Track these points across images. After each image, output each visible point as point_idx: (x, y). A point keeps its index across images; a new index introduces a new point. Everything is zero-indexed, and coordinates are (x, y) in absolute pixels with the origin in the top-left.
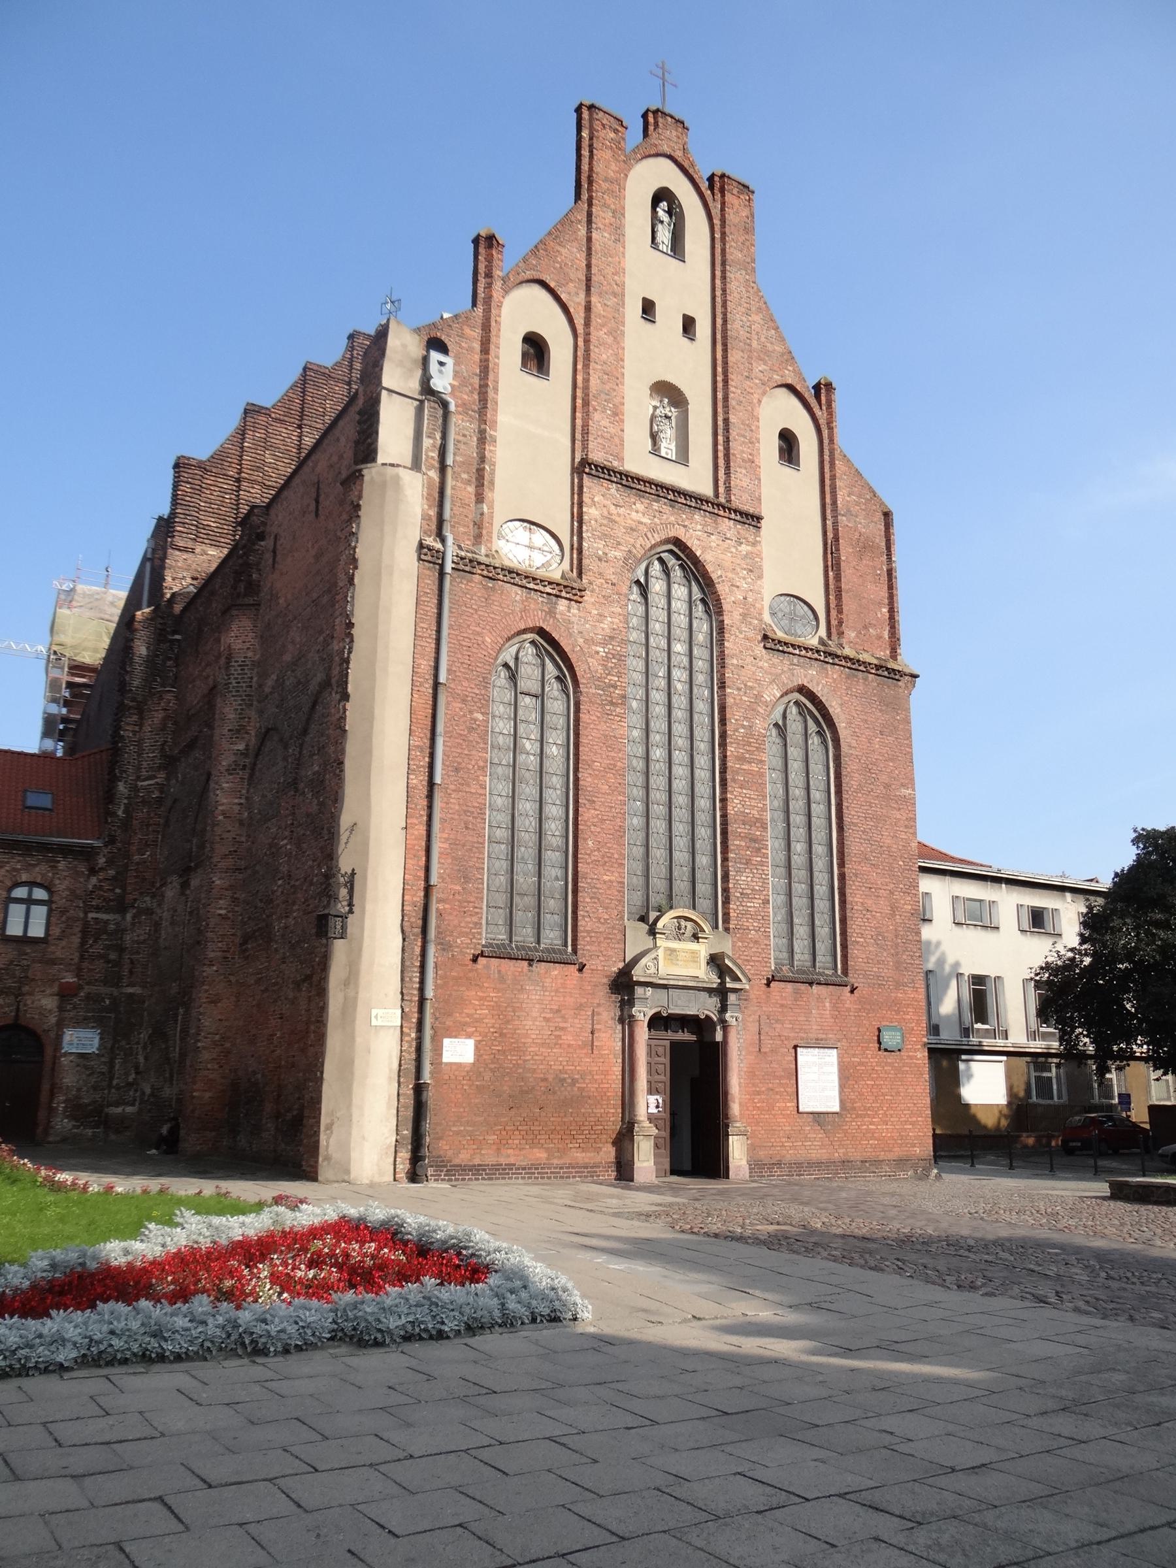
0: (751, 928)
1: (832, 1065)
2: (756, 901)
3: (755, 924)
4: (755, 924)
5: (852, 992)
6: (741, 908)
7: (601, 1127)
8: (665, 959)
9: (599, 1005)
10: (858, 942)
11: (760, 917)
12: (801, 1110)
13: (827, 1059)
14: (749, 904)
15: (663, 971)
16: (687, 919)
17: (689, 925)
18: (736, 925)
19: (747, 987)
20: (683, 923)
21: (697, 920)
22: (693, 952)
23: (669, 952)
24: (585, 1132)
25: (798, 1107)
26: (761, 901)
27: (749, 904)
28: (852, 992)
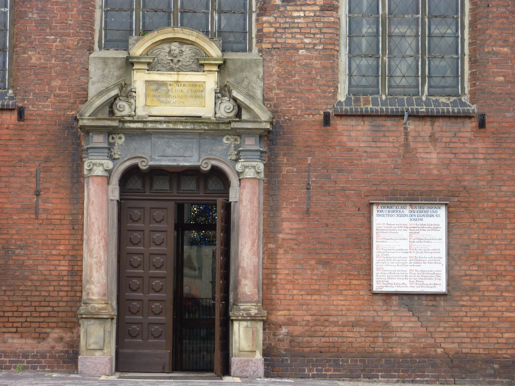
0: (298, 46)
1: (436, 228)
2: (309, 8)
3: (307, 41)
4: (307, 41)
5: (482, 125)
6: (282, 21)
7: (49, 309)
8: (147, 96)
9: (47, 160)
10: (496, 54)
11: (312, 31)
12: (376, 288)
13: (427, 220)
14: (295, 14)
15: (141, 112)
16: (182, 41)
17: (185, 48)
18: (273, 44)
19: (268, 126)
20: (175, 47)
21: (198, 41)
22: (194, 84)
23: (154, 87)
24: (25, 314)
25: (371, 285)
26: (317, 8)
27: (295, 14)
28: (482, 125)
